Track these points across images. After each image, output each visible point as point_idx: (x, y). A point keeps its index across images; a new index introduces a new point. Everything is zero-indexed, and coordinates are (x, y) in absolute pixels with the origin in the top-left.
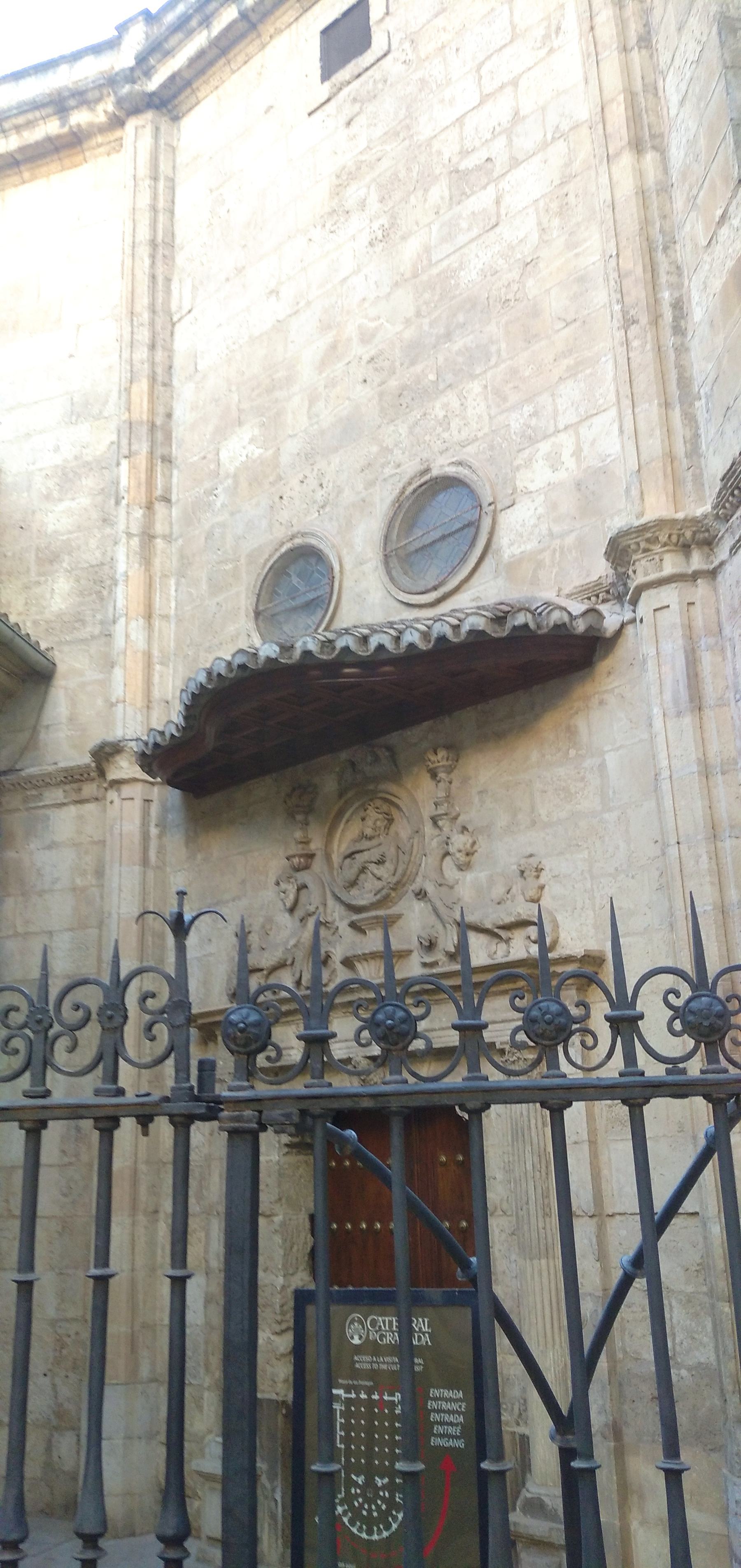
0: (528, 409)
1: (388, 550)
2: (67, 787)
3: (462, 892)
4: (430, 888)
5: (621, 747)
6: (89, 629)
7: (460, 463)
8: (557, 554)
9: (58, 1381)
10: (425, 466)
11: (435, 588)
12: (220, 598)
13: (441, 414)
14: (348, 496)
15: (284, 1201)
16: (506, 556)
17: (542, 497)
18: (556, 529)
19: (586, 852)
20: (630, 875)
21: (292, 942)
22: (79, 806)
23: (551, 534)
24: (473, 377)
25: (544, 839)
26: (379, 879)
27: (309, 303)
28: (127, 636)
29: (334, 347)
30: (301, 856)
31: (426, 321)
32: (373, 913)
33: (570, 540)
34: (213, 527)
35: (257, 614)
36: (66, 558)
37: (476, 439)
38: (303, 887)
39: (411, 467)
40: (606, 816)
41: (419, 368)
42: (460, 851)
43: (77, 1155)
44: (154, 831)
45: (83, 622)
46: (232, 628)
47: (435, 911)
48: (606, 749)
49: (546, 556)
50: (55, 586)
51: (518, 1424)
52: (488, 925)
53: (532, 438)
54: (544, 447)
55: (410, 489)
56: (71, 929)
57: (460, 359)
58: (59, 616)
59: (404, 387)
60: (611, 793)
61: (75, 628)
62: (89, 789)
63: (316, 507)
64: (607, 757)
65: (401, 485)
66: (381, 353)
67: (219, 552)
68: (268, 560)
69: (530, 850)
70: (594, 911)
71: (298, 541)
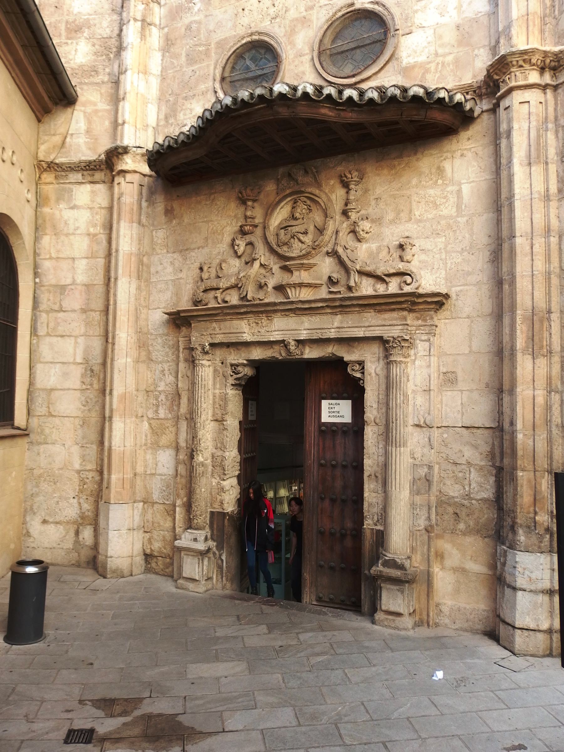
1: (321, 49)
2: (85, 173)
3: (359, 254)
4: (340, 250)
5: (473, 182)
6: (100, 77)
7: (377, 3)
8: (440, 66)
9: (82, 501)
11: (353, 76)
12: (195, 67)
14: (292, 14)
15: (230, 414)
16: (404, 63)
18: (440, 51)
19: (444, 238)
20: (471, 253)
22: (92, 185)
25: (416, 229)
26: (302, 243)
28: (132, 83)
30: (251, 226)
32: (299, 262)
33: (450, 58)
34: (191, 22)
35: (223, 79)
36: (86, 30)
40: (459, 219)
42: (363, 231)
43: (91, 385)
44: (144, 204)
45: (97, 72)
46: (203, 87)
47: (341, 263)
48: (462, 182)
49: (433, 66)
50: (78, 47)
51: (376, 525)
52: (379, 273)
55: (340, 14)
56: (87, 258)
58: (81, 66)
60: (463, 207)
61: (91, 75)
62: (98, 176)
63: (269, 18)
64: (463, 186)
67: (195, 39)
68: (232, 47)
69: (407, 234)
70: (446, 271)
71: (255, 37)
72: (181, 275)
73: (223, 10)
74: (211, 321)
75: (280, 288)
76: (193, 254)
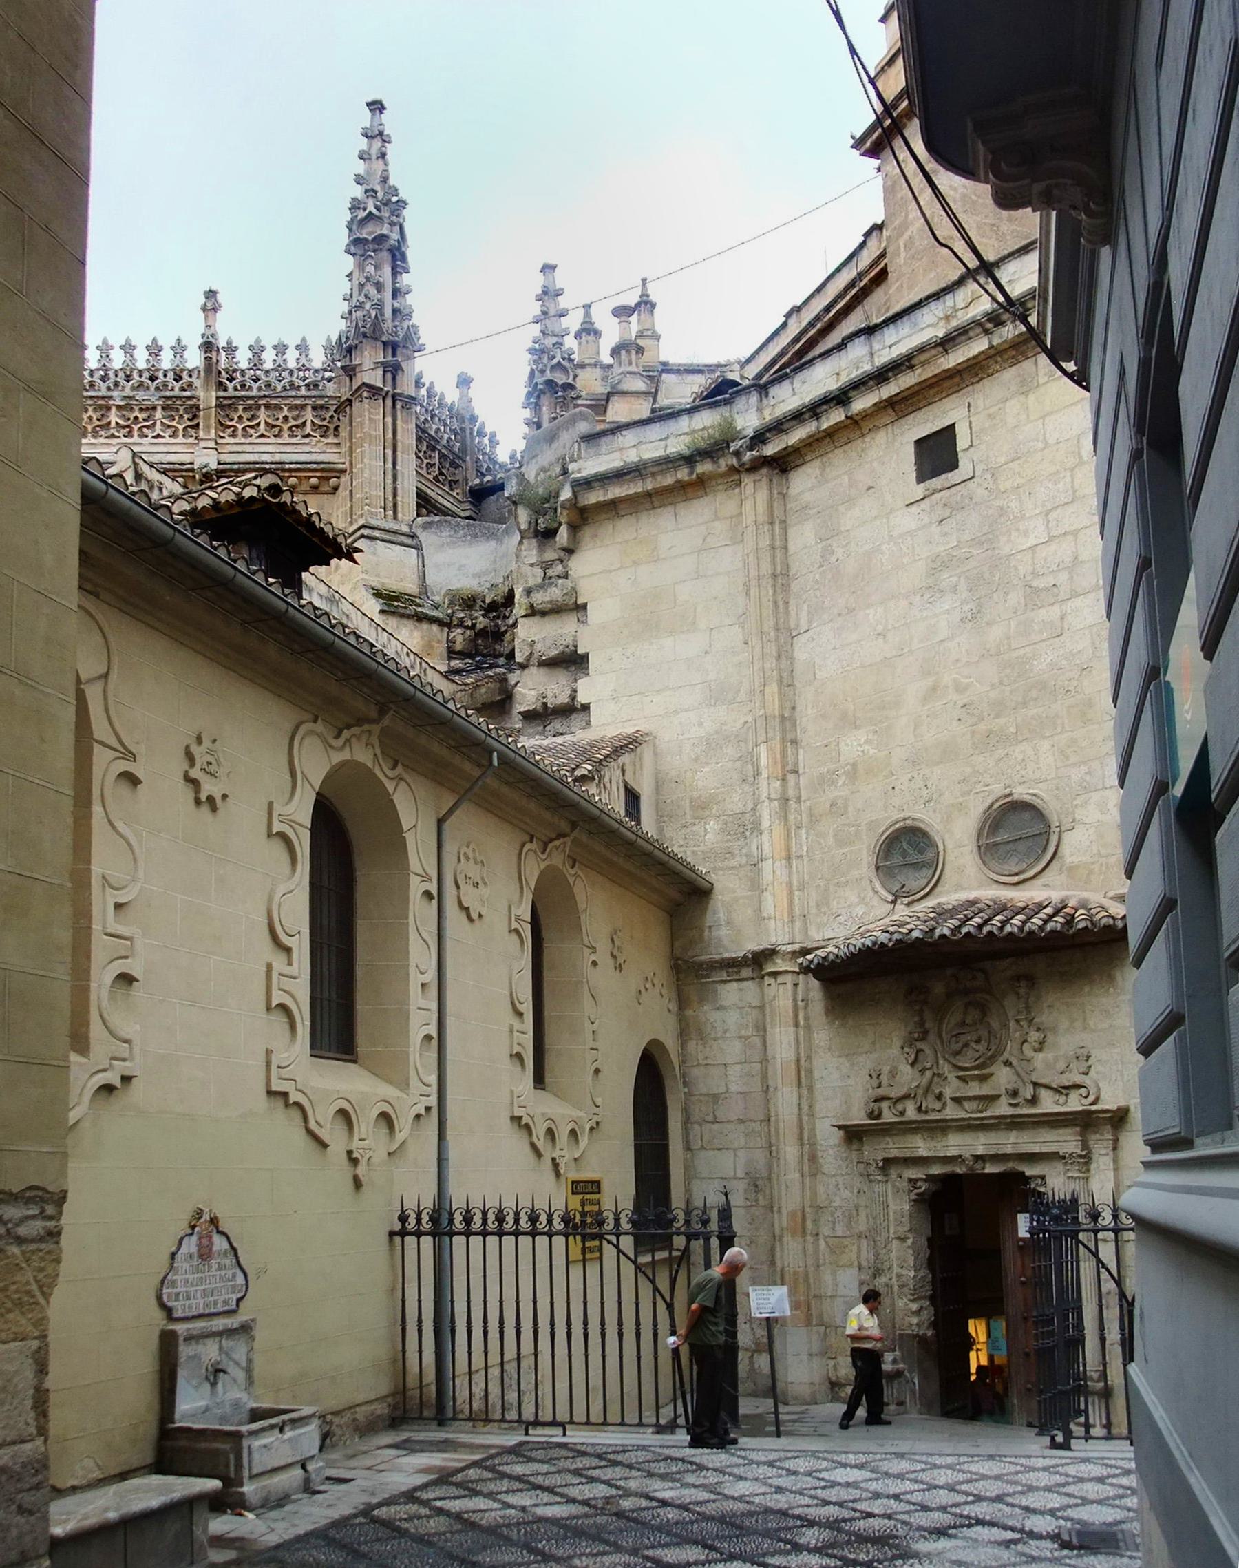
0: (1084, 768)
10: (1007, 791)
11: (1017, 874)
13: (1020, 757)
17: (1093, 829)
21: (914, 1084)
23: (1099, 853)
24: (1045, 738)
27: (911, 652)
29: (934, 689)
31: (1008, 689)
37: (1046, 780)
38: (919, 1051)
39: (998, 789)
41: (1002, 721)
53: (1087, 788)
54: (1096, 797)
57: (1034, 723)
59: (991, 732)
65: (989, 801)
66: (972, 703)
72: (850, 1082)
73: (871, 786)
74: (884, 1136)
75: (957, 1100)
76: (861, 1059)
